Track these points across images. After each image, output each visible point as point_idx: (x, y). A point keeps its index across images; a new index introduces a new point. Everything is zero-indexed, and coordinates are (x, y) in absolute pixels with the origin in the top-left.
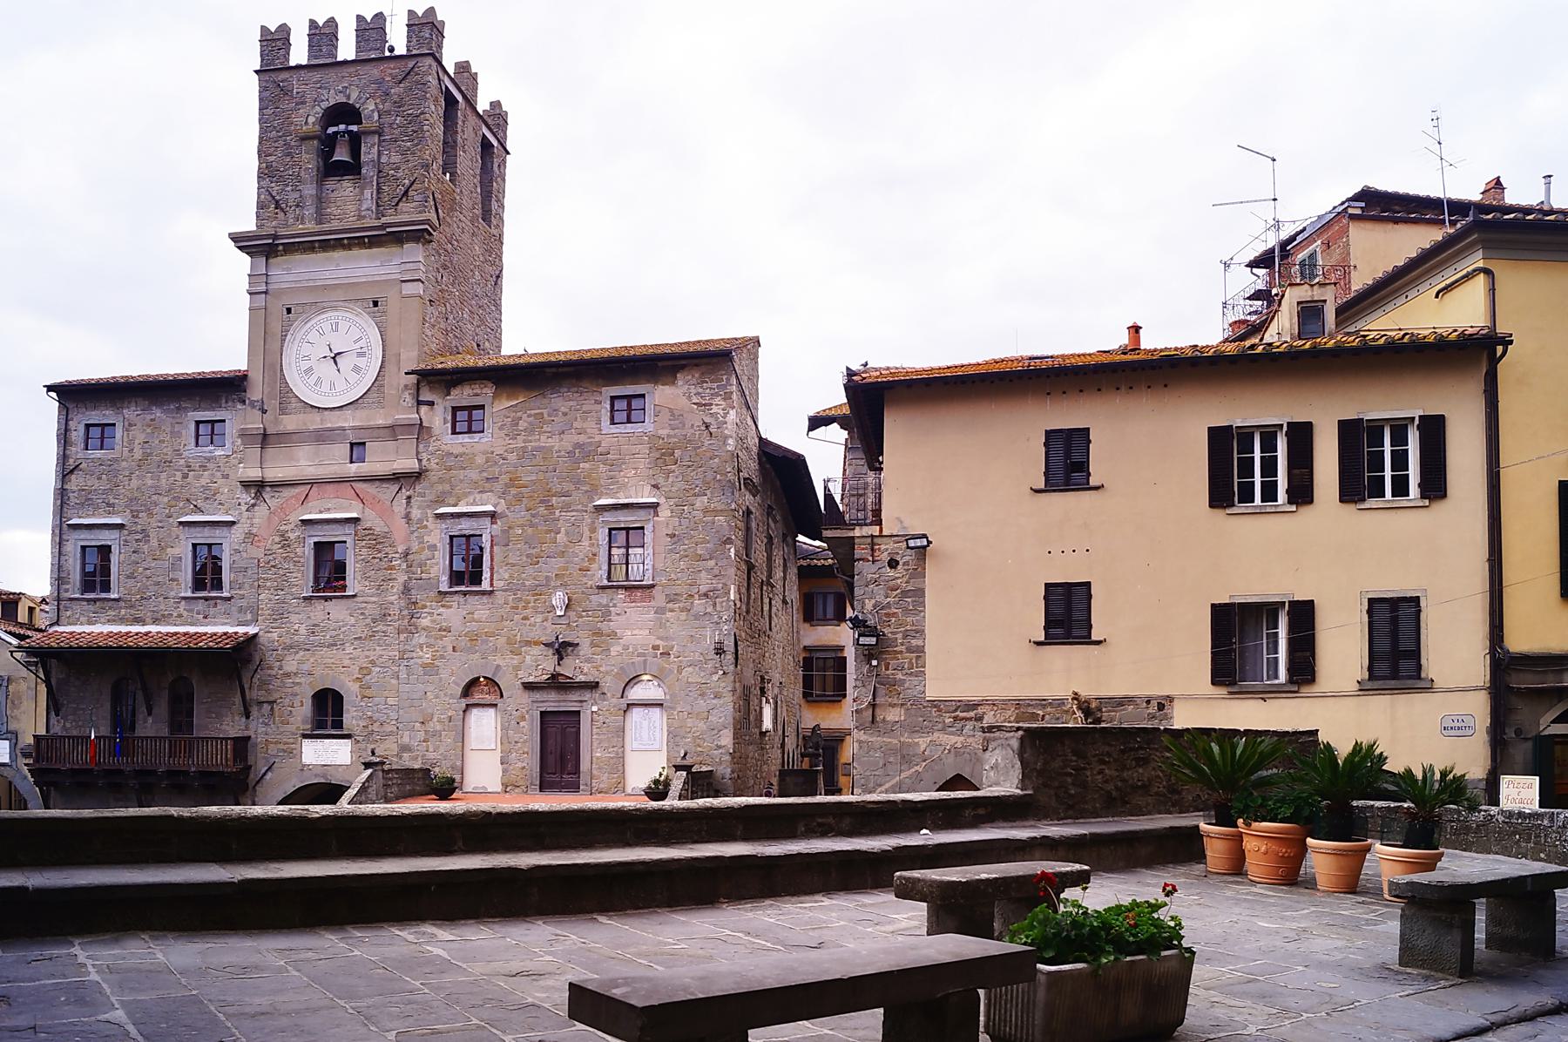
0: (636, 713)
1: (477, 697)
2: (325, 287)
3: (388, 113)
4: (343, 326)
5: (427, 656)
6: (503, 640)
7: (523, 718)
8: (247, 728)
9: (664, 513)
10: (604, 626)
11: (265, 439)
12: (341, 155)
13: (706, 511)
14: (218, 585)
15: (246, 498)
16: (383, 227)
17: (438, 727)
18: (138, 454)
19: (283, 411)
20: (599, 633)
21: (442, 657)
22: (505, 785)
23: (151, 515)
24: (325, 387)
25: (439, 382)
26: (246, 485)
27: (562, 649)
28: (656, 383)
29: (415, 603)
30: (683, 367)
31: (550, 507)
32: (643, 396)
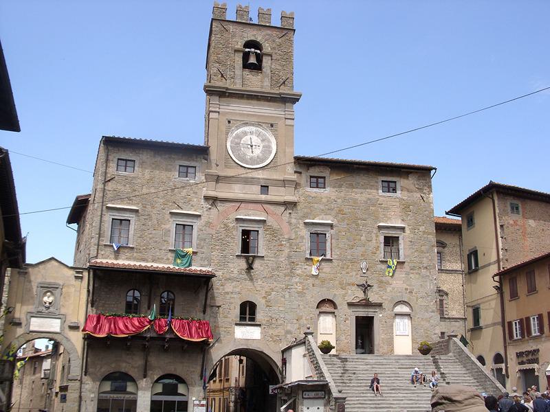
0: (398, 320)
1: (324, 309)
2: (248, 115)
3: (274, 48)
5: (300, 288)
7: (347, 319)
9: (407, 231)
10: (384, 279)
11: (218, 179)
12: (252, 60)
16: (280, 94)
20: (381, 282)
21: (307, 289)
23: (153, 207)
25: (304, 164)
26: (207, 198)
27: (366, 288)
28: (401, 177)
29: (293, 263)
30: (411, 173)
31: (357, 225)
32: (395, 182)
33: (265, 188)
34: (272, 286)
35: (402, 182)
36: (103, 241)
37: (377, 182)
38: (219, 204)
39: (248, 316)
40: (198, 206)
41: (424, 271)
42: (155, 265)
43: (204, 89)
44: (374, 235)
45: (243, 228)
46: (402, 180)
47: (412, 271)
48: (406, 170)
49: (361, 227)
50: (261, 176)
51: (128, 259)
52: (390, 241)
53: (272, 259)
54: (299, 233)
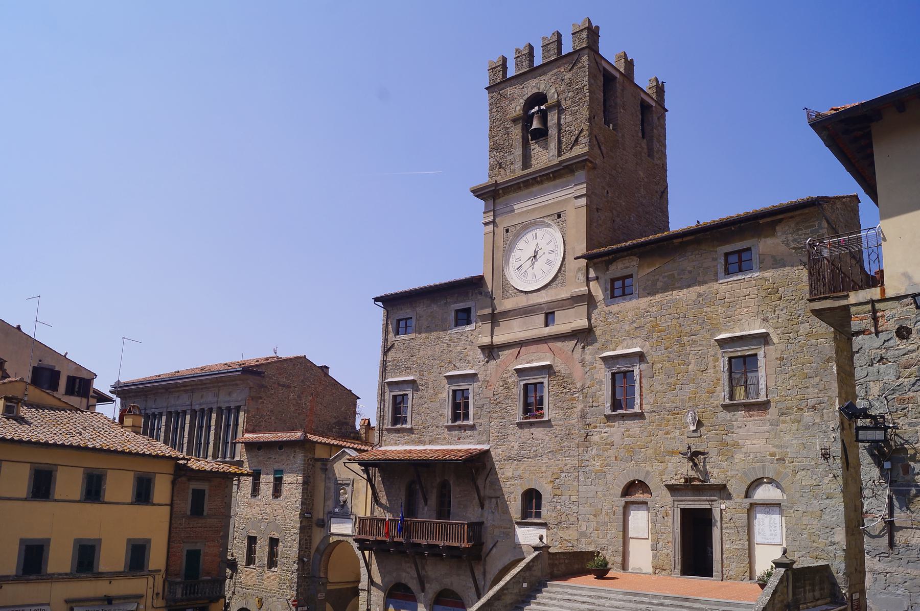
2: (528, 212)
5: (597, 464)
6: (650, 451)
8: (482, 516)
10: (728, 438)
11: (495, 319)
14: (466, 417)
17: (606, 519)
19: (504, 297)
21: (607, 465)
22: (655, 568)
26: (483, 348)
29: (589, 425)
30: (780, 221)
31: (684, 345)
32: (749, 249)
33: (549, 318)
34: (561, 464)
35: (765, 245)
37: (715, 259)
40: (474, 364)
41: (807, 416)
42: (429, 447)
43: (477, 196)
44: (711, 359)
46: (763, 240)
47: (783, 418)
48: (769, 219)
50: (542, 301)
51: (406, 443)
52: (742, 366)
53: (561, 423)
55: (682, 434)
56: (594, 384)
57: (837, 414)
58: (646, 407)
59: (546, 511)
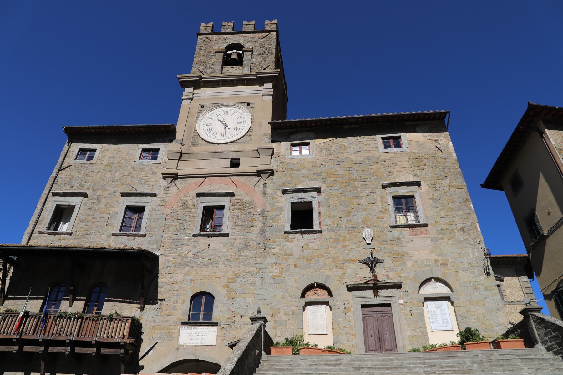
2: (223, 98)
4: (230, 113)
6: (329, 260)
7: (349, 310)
10: (398, 249)
13: (449, 186)
15: (165, 183)
17: (285, 318)
18: (105, 162)
19: (193, 144)
20: (396, 253)
23: (105, 191)
24: (218, 136)
26: (165, 176)
27: (372, 263)
30: (419, 125)
31: (354, 187)
32: (400, 137)
36: (39, 228)
38: (178, 182)
39: (202, 313)
41: (459, 235)
45: (205, 204)
47: (441, 236)
49: (359, 190)
50: (232, 149)
52: (404, 203)
53: (241, 237)
54: (276, 204)
55: (359, 247)
56: (274, 210)
57: (480, 233)
58: (324, 228)
59: (217, 313)
